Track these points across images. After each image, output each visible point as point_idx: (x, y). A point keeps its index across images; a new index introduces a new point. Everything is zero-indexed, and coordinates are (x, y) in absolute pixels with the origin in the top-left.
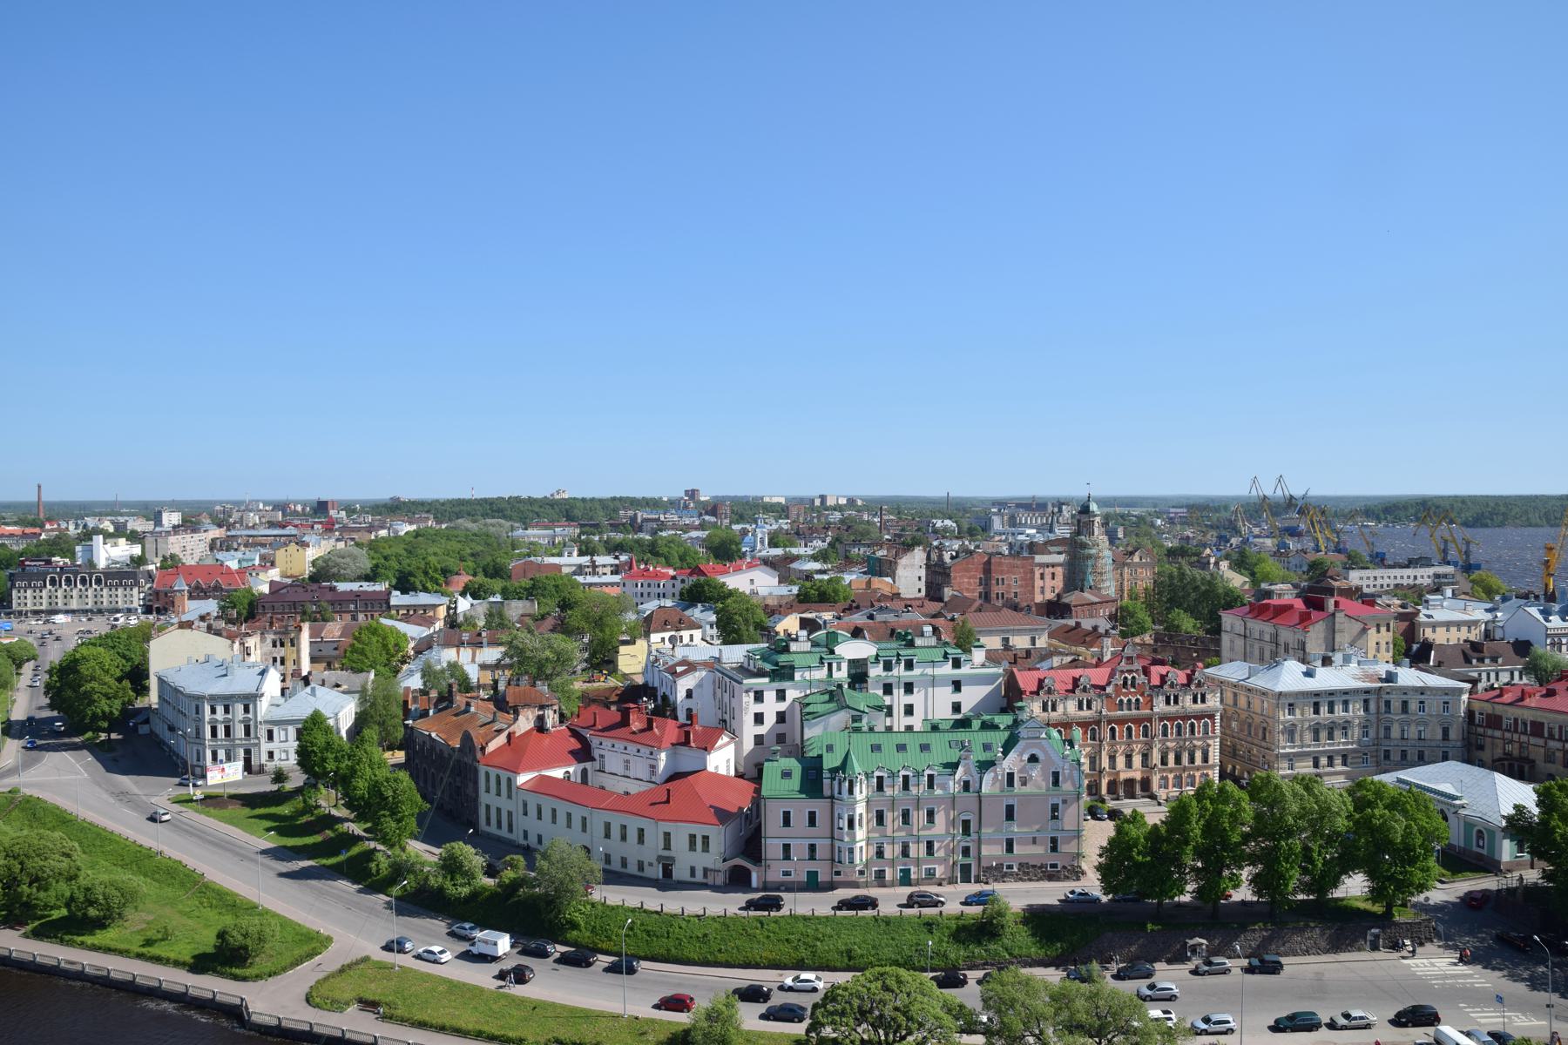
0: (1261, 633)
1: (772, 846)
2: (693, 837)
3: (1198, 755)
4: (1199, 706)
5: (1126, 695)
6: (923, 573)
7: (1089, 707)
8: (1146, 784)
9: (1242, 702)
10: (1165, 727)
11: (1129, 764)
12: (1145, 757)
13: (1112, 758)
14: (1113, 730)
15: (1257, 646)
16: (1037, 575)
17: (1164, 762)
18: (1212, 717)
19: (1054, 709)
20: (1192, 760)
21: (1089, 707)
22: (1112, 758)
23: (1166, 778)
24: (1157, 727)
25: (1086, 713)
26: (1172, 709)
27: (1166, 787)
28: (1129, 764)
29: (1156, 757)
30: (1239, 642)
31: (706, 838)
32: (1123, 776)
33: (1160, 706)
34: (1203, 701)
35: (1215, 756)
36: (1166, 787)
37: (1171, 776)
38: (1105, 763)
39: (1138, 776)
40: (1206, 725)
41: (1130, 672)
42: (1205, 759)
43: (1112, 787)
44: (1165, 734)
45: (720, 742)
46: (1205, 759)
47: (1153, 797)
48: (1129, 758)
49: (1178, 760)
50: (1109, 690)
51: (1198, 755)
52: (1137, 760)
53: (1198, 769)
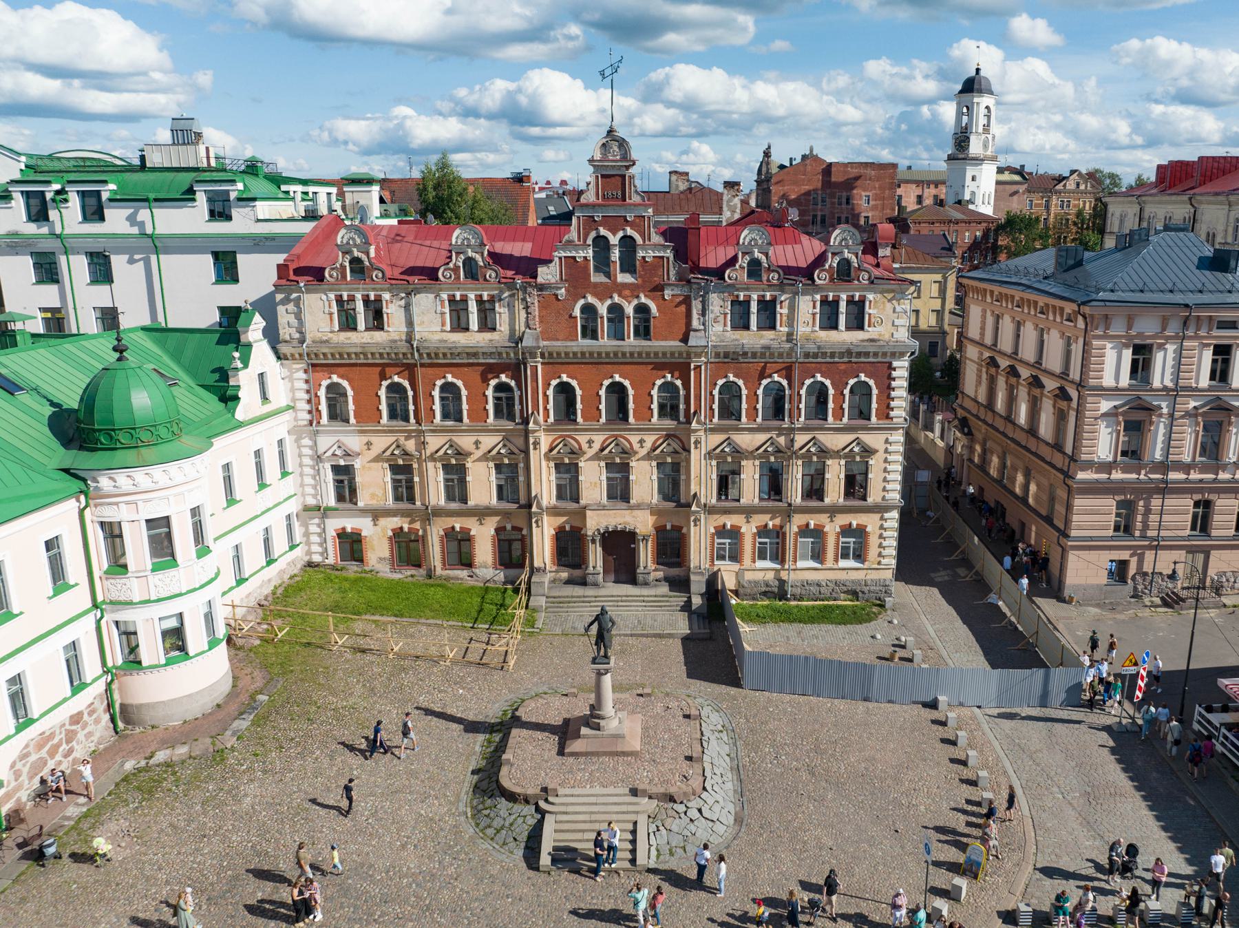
3: (835, 475)
4: (843, 337)
5: (603, 292)
7: (487, 325)
10: (731, 392)
14: (565, 391)
20: (815, 490)
21: (487, 325)
24: (705, 391)
25: (475, 338)
26: (754, 338)
27: (735, 557)
32: (595, 523)
33: (715, 328)
36: (735, 557)
37: (748, 529)
40: (862, 391)
42: (855, 485)
50: (547, 274)
51: (835, 475)
53: (833, 511)
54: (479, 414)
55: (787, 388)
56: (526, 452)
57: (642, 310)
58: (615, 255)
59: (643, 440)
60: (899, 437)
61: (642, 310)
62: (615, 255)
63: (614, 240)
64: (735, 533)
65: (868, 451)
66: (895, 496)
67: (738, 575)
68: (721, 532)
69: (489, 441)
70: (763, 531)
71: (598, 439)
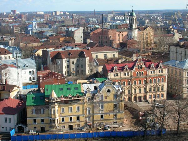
0: (181, 51)
1: (30, 120)
2: (6, 118)
4: (161, 73)
5: (139, 71)
6: (82, 35)
7: (128, 75)
8: (145, 97)
9: (174, 72)
11: (140, 92)
12: (145, 89)
13: (135, 90)
14: (135, 81)
15: (180, 56)
16: (117, 35)
17: (150, 91)
18: (165, 77)
19: (117, 75)
20: (159, 90)
21: (128, 75)
22: (135, 90)
23: (151, 95)
25: (127, 76)
26: (153, 74)
27: (151, 98)
28: (140, 92)
29: (148, 89)
30: (175, 54)
31: (10, 119)
32: (138, 95)
34: (162, 72)
35: (165, 88)
36: (151, 98)
37: (152, 95)
38: (133, 91)
39: (142, 95)
41: (140, 64)
42: (162, 89)
43: (135, 98)
44: (150, 82)
45: (14, 89)
46: (162, 89)
47: (147, 101)
48: (140, 89)
49: (154, 90)
52: (142, 90)
53: (161, 92)
54: (127, 85)
55: (156, 79)
56: (131, 88)
57: (142, 72)
58: (140, 67)
59: (142, 86)
60: (166, 83)
61: (142, 72)
62: (140, 67)
63: (140, 66)
64: (151, 95)
65: (164, 85)
66: (166, 90)
67: (151, 100)
68: (150, 95)
69: (128, 87)
70: (154, 95)
71: (138, 86)
